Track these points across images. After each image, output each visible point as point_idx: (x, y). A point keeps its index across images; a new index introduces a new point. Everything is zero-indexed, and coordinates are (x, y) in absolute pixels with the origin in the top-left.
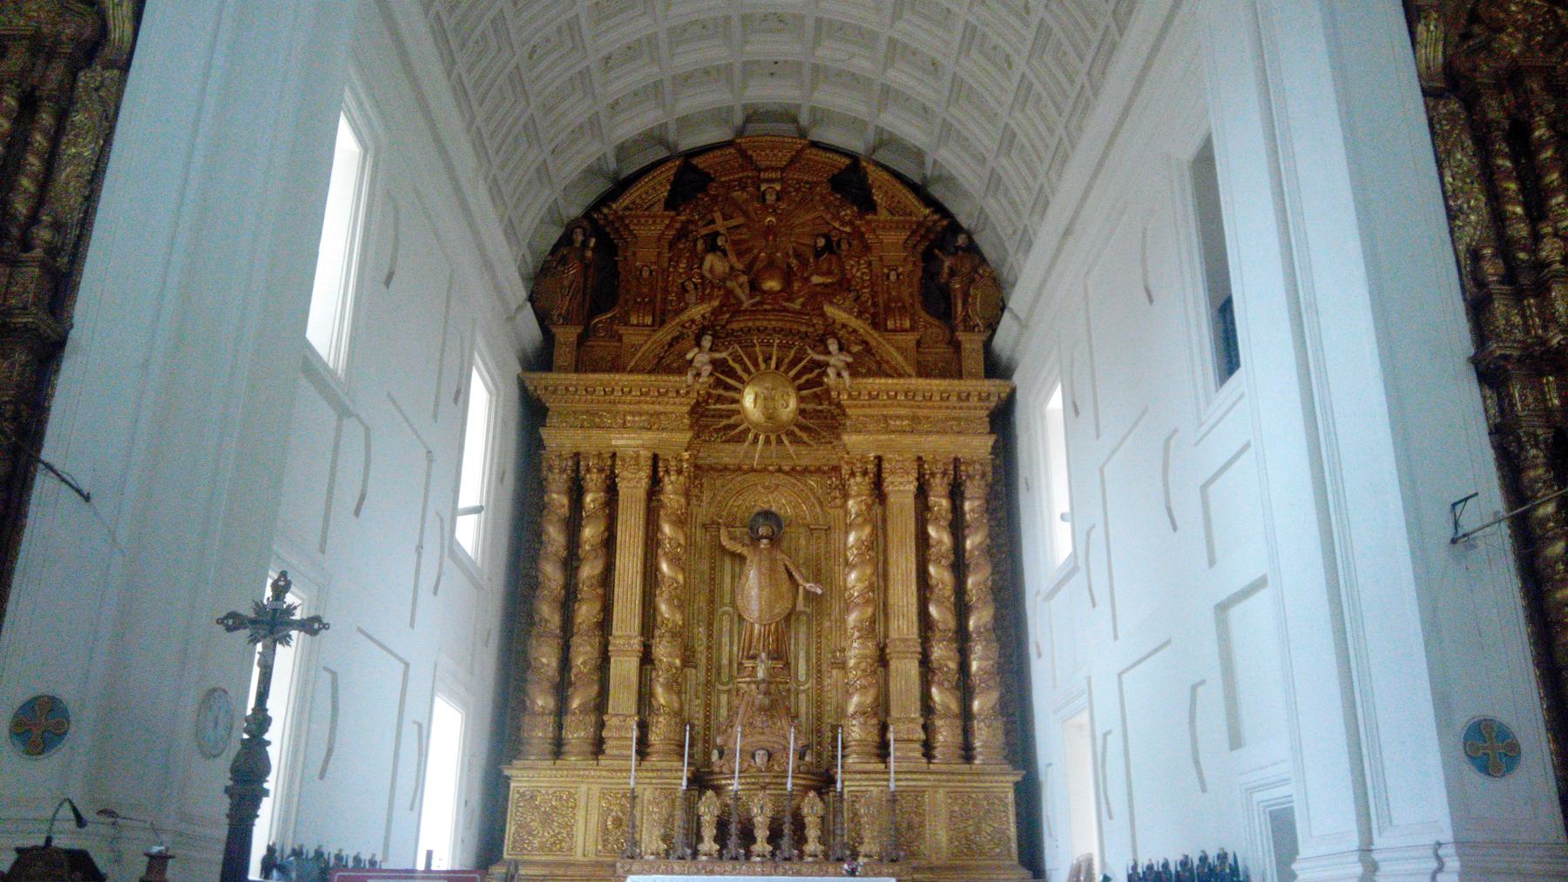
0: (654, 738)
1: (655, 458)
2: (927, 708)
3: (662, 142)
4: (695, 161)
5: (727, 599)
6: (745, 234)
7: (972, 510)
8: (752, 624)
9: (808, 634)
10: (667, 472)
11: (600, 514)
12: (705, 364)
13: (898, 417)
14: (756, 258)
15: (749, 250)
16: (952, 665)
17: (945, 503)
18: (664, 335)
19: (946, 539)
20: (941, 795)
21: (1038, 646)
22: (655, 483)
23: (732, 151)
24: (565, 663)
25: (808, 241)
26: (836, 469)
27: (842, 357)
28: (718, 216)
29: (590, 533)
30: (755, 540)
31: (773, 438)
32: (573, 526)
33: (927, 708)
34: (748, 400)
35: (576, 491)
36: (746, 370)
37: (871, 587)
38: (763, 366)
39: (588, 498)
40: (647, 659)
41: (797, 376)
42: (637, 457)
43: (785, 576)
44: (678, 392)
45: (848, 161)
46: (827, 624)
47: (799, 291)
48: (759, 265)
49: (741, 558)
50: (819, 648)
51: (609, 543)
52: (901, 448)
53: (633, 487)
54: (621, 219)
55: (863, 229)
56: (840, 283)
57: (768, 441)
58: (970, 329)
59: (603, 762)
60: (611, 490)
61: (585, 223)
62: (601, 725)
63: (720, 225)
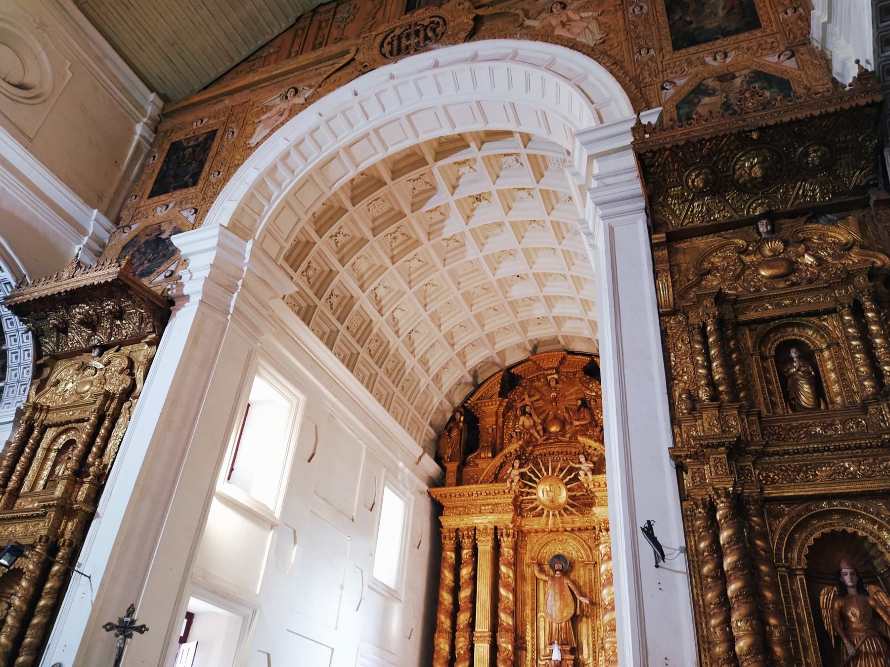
1: (496, 528)
3: (494, 364)
6: (541, 403)
9: (588, 628)
10: (502, 535)
11: (469, 561)
14: (548, 415)
15: (544, 411)
18: (498, 460)
23: (530, 363)
24: (453, 648)
25: (573, 403)
26: (594, 528)
27: (586, 465)
29: (465, 572)
31: (557, 512)
35: (458, 549)
38: (545, 474)
39: (465, 552)
42: (486, 528)
43: (569, 593)
44: (504, 491)
45: (589, 359)
50: (594, 638)
51: (474, 578)
53: (485, 547)
54: (477, 404)
56: (590, 423)
60: (475, 549)
61: (462, 410)
63: (527, 401)
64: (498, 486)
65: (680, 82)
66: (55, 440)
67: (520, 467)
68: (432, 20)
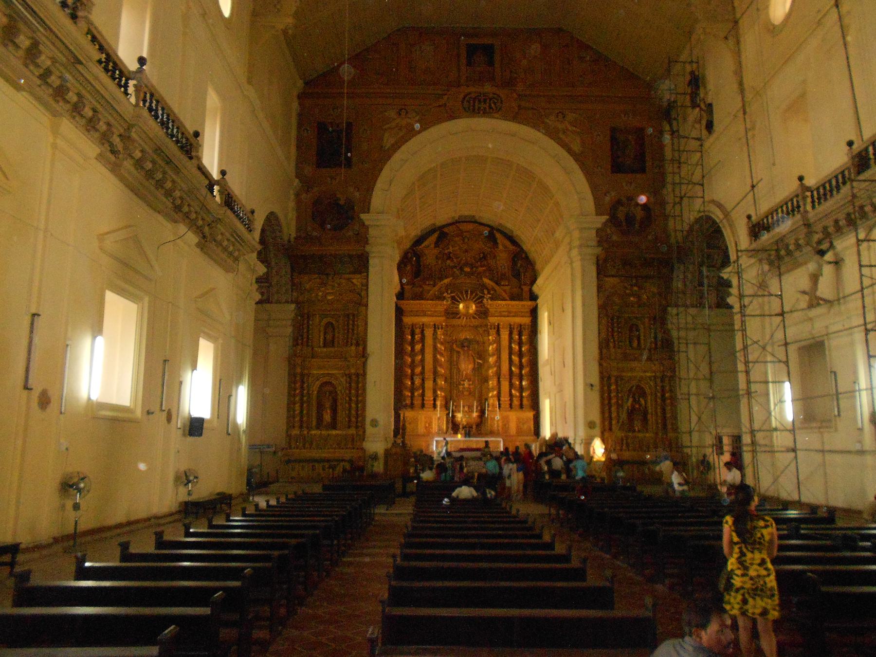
1: (435, 325)
2: (511, 395)
4: (443, 230)
13: (504, 311)
16: (517, 383)
17: (517, 337)
19: (517, 347)
20: (514, 417)
22: (435, 331)
26: (486, 325)
28: (451, 248)
29: (418, 347)
30: (463, 346)
32: (412, 344)
33: (511, 395)
34: (461, 306)
37: (496, 362)
38: (465, 298)
39: (416, 336)
40: (435, 381)
41: (476, 301)
46: (483, 370)
48: (462, 262)
49: (458, 352)
51: (422, 351)
52: (504, 321)
53: (429, 333)
57: (467, 318)
58: (525, 284)
60: (422, 332)
61: (411, 251)
62: (423, 400)
64: (440, 302)
65: (613, 194)
66: (320, 322)
67: (451, 293)
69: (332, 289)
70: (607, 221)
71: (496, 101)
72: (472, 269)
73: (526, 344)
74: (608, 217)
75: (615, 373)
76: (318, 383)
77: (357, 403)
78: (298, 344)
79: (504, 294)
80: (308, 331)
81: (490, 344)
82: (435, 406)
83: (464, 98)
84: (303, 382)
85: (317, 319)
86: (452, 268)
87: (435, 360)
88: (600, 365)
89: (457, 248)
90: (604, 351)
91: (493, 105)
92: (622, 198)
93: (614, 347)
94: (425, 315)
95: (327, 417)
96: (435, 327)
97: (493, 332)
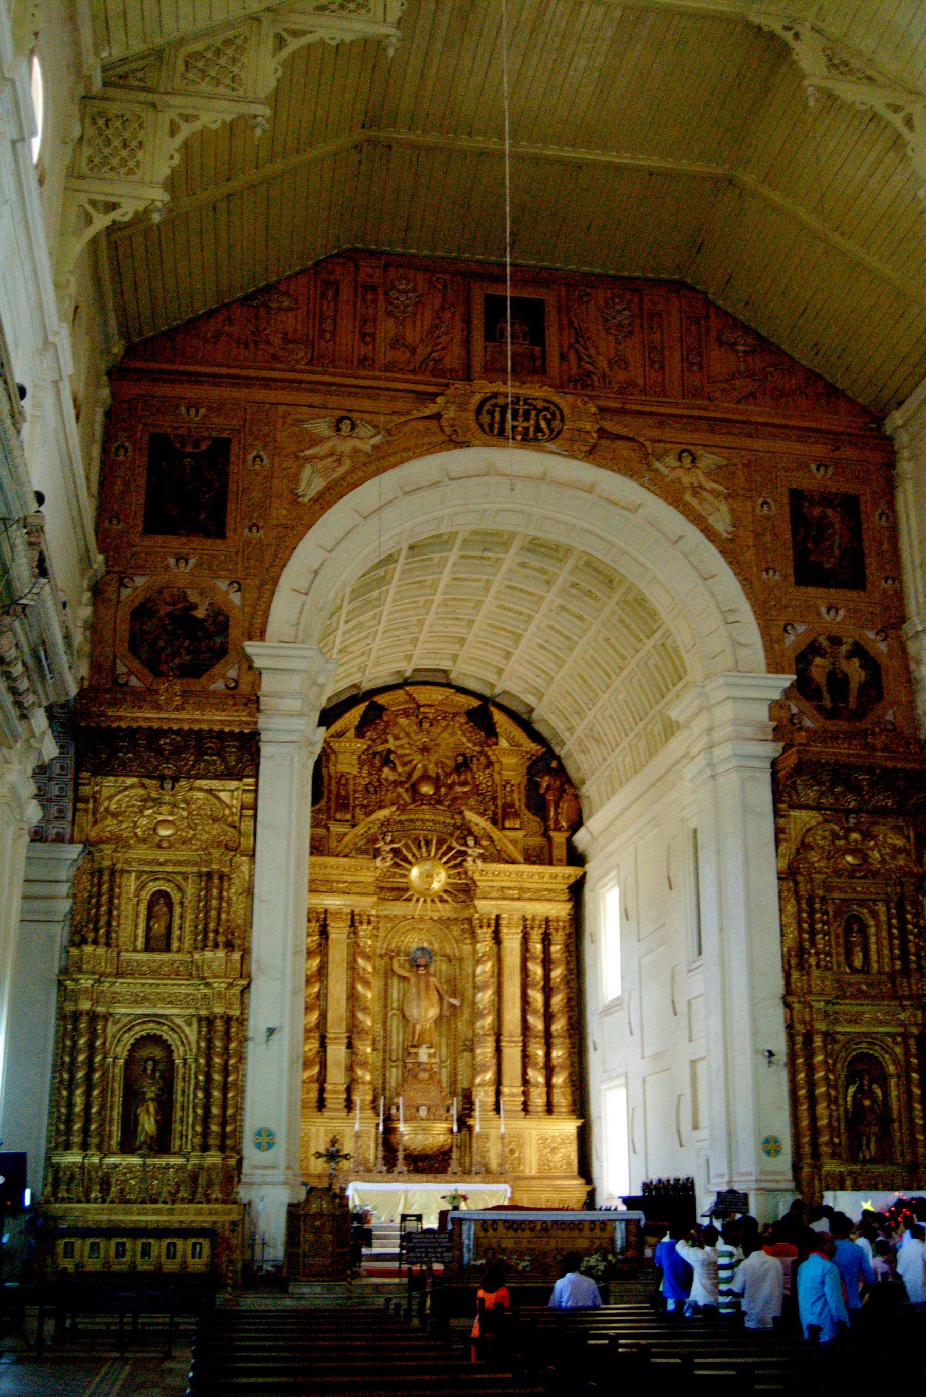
0: (357, 1098)
1: (353, 912)
2: (526, 1082)
4: (375, 699)
5: (395, 1005)
7: (556, 952)
8: (414, 1026)
12: (388, 852)
13: (510, 888)
15: (410, 762)
21: (594, 1043)
26: (469, 920)
28: (390, 738)
34: (415, 872)
36: (414, 855)
47: (446, 795)
49: (405, 979)
52: (512, 910)
55: (490, 753)
57: (425, 901)
58: (558, 829)
59: (326, 1113)
62: (322, 1090)
65: (801, 628)
67: (392, 842)
68: (546, 405)
69: (171, 814)
70: (792, 685)
71: (549, 416)
72: (437, 789)
73: (559, 966)
74: (795, 677)
75: (821, 1026)
76: (129, 1039)
77: (225, 1089)
78: (84, 941)
79: (511, 847)
80: (109, 912)
81: (478, 962)
82: (349, 1105)
83: (484, 402)
84: (93, 1035)
85: (130, 884)
86: (396, 784)
87: (353, 996)
88: (788, 1006)
89: (405, 741)
90: (795, 975)
91: (543, 424)
92: (822, 640)
93: (818, 966)
94: (331, 891)
95: (148, 1124)
96: (354, 921)
97: (485, 934)
